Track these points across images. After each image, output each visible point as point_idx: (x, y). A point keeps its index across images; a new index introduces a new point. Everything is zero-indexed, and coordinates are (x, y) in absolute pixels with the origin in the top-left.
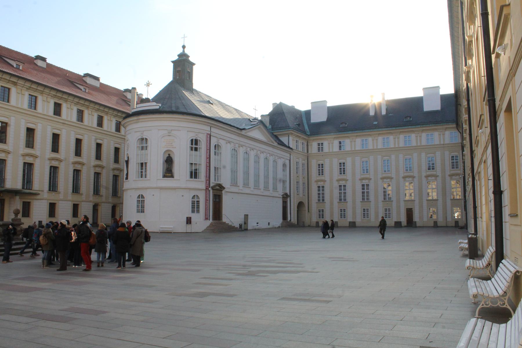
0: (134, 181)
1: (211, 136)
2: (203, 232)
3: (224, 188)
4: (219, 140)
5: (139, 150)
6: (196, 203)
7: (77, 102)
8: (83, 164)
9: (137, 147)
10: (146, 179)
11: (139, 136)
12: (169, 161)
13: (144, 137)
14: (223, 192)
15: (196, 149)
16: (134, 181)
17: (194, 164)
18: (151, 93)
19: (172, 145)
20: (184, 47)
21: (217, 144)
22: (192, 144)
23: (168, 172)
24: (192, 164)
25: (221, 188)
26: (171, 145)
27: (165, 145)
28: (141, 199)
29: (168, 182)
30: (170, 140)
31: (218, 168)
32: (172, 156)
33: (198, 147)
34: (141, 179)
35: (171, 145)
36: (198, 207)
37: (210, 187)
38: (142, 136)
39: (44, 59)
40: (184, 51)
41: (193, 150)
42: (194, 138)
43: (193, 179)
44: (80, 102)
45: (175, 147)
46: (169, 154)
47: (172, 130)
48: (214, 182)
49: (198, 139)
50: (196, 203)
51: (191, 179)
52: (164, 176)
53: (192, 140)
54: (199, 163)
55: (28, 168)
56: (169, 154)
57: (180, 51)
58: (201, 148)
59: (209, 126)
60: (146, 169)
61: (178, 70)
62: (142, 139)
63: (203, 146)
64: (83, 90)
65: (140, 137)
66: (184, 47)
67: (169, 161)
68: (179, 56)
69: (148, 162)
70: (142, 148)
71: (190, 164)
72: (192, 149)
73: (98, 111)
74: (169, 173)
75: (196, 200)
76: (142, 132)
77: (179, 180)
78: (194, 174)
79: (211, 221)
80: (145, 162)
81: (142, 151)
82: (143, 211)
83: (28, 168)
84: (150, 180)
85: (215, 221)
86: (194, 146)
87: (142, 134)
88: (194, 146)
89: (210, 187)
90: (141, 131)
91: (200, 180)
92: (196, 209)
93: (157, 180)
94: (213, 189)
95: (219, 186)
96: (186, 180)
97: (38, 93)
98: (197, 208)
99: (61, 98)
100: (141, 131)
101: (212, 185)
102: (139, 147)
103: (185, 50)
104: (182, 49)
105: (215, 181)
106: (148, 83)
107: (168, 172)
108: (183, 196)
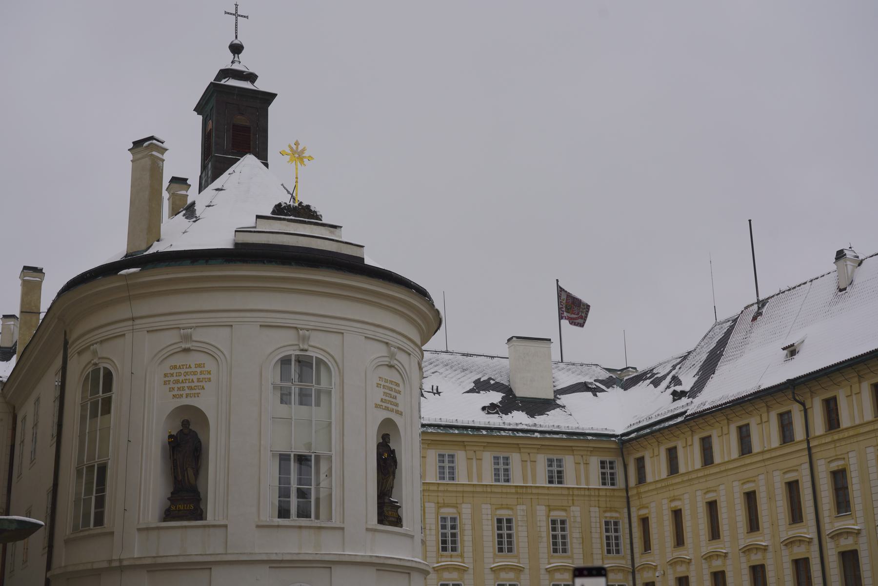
0: (258, 526)
16: (258, 526)
19: (397, 405)
20: (236, 49)
26: (393, 400)
27: (382, 400)
30: (391, 382)
32: (392, 446)
34: (303, 522)
35: (393, 400)
38: (302, 350)
47: (399, 348)
62: (304, 362)
65: (294, 352)
66: (236, 49)
69: (330, 458)
70: (304, 398)
76: (307, 333)
84: (343, 529)
87: (305, 339)
90: (302, 329)
100: (302, 329)
104: (230, 56)
106: (294, 147)
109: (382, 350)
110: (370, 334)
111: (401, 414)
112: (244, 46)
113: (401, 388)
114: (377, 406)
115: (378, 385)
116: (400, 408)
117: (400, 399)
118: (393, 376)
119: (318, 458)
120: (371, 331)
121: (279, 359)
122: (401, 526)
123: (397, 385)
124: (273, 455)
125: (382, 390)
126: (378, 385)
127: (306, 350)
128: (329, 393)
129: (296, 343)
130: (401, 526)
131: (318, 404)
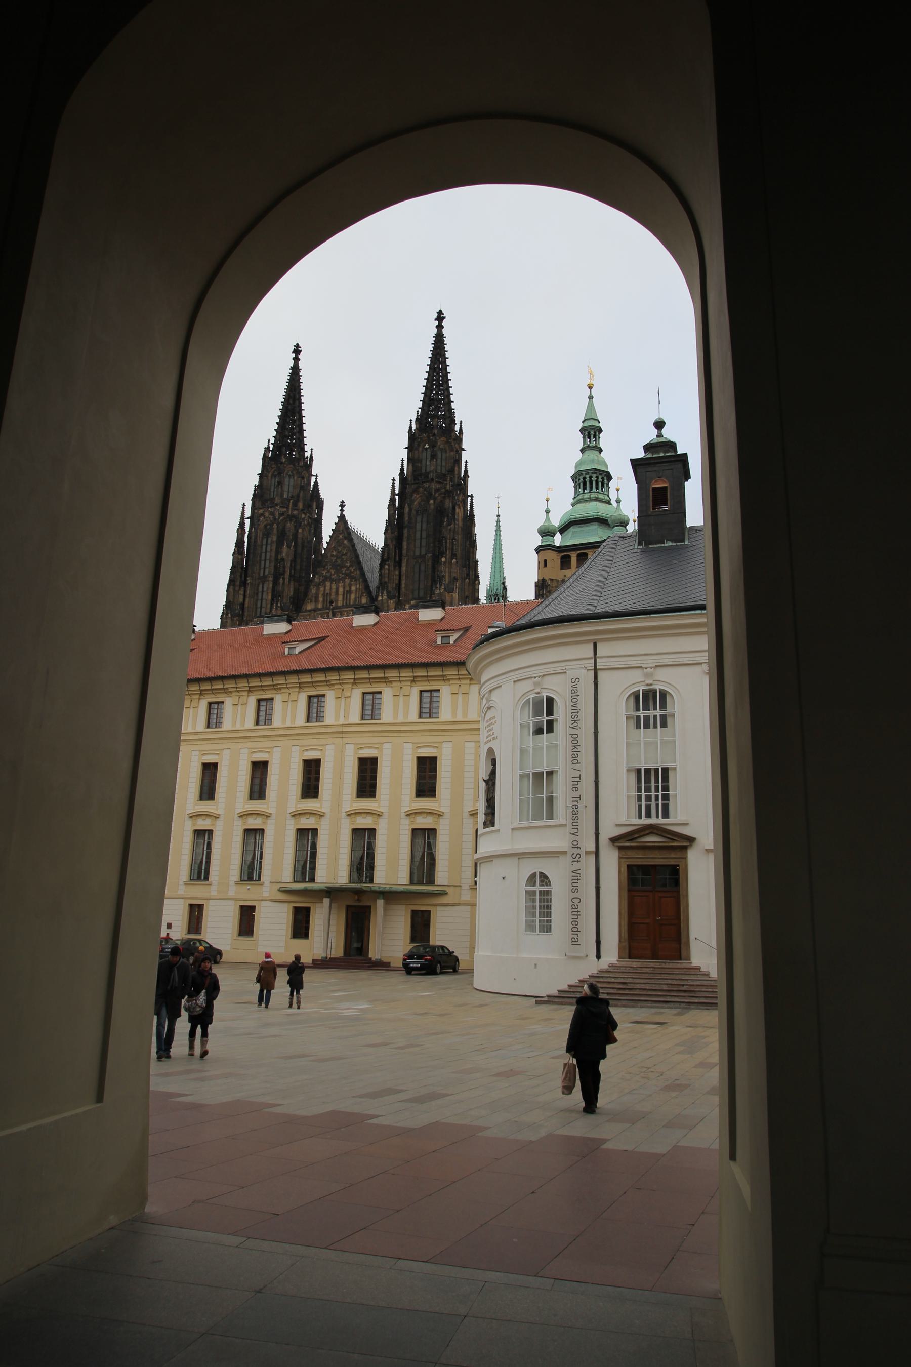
5: (638, 726)
9: (627, 718)
11: (636, 682)
13: (657, 687)
20: (659, 425)
38: (647, 685)
40: (659, 436)
57: (651, 435)
60: (666, 788)
61: (654, 486)
65: (641, 688)
66: (659, 425)
68: (648, 448)
69: (675, 769)
80: (666, 765)
81: (651, 730)
87: (651, 675)
90: (646, 668)
102: (638, 718)
103: (664, 431)
112: (666, 422)
119: (666, 771)
121: (631, 694)
124: (628, 770)
127: (651, 685)
128: (673, 716)
129: (643, 680)
131: (664, 724)
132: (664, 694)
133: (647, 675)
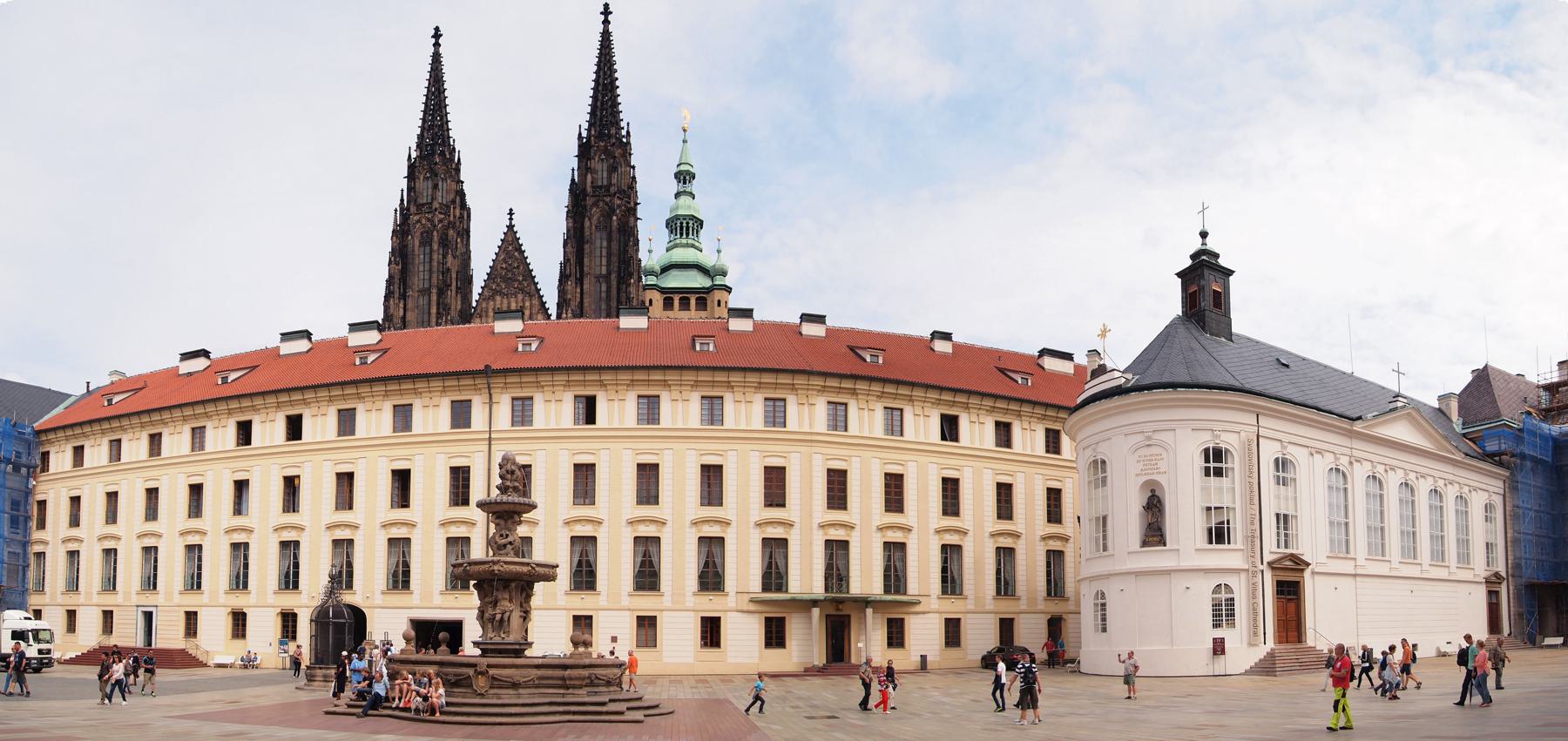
1: (1260, 439)
2: (1247, 673)
3: (1308, 564)
4: (1284, 448)
6: (1224, 602)
7: (991, 407)
8: (1016, 536)
10: (1105, 553)
12: (1154, 505)
13: (1098, 457)
14: (1307, 574)
15: (1219, 473)
17: (1215, 508)
18: (1121, 357)
21: (1280, 456)
22: (1207, 461)
23: (1154, 534)
24: (1209, 509)
25: (1299, 564)
27: (1142, 470)
28: (1100, 601)
29: (1155, 559)
31: (1286, 516)
33: (1223, 465)
36: (1231, 614)
37: (1262, 564)
38: (1095, 456)
39: (947, 336)
41: (1210, 476)
42: (1211, 446)
43: (1214, 546)
44: (997, 405)
45: (1165, 472)
46: (1153, 491)
47: (1154, 431)
48: (1274, 549)
49: (1223, 446)
50: (1224, 602)
51: (1211, 546)
52: (1145, 544)
53: (1206, 451)
54: (1231, 505)
55: (895, 552)
56: (1153, 491)
58: (1233, 469)
59: (1254, 412)
62: (1095, 462)
63: (1235, 464)
64: (1020, 382)
67: (1154, 505)
71: (1205, 511)
72: (1207, 472)
73: (1044, 419)
74: (1153, 536)
75: (1224, 596)
77: (1178, 550)
78: (1219, 535)
79: (1271, 644)
82: (1104, 630)
83: (895, 552)
85: (1283, 646)
86: (1212, 465)
87: (1094, 450)
88: (1212, 465)
89: (1265, 563)
91: (1232, 546)
92: (1224, 618)
93: (1129, 553)
94: (1273, 569)
95: (1291, 560)
96: (1197, 550)
97: (903, 402)
98: (1227, 615)
99: (953, 404)
101: (1268, 558)
105: (1278, 547)
107: (1154, 534)
108: (1188, 588)
109: (1139, 438)
110: (1126, 432)
111: (1165, 472)
113: (1164, 455)
114: (1137, 475)
115: (1138, 462)
116: (1162, 470)
117: (1160, 464)
118: (1154, 450)
120: (1126, 430)
122: (1165, 545)
123: (1157, 455)
125: (1142, 463)
126: (1138, 462)
130: (1165, 545)
132: (1103, 462)
133: (1094, 450)
